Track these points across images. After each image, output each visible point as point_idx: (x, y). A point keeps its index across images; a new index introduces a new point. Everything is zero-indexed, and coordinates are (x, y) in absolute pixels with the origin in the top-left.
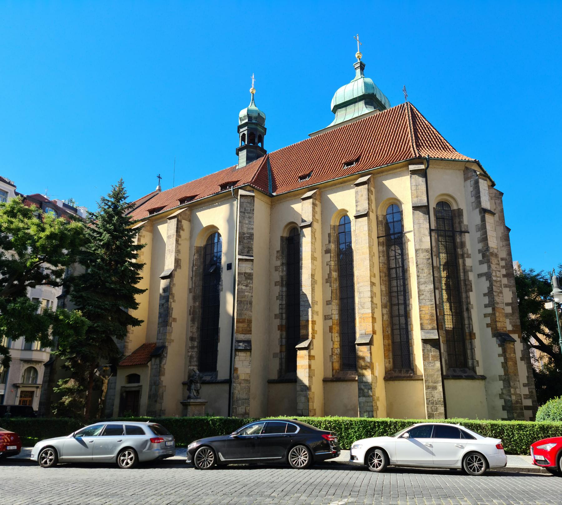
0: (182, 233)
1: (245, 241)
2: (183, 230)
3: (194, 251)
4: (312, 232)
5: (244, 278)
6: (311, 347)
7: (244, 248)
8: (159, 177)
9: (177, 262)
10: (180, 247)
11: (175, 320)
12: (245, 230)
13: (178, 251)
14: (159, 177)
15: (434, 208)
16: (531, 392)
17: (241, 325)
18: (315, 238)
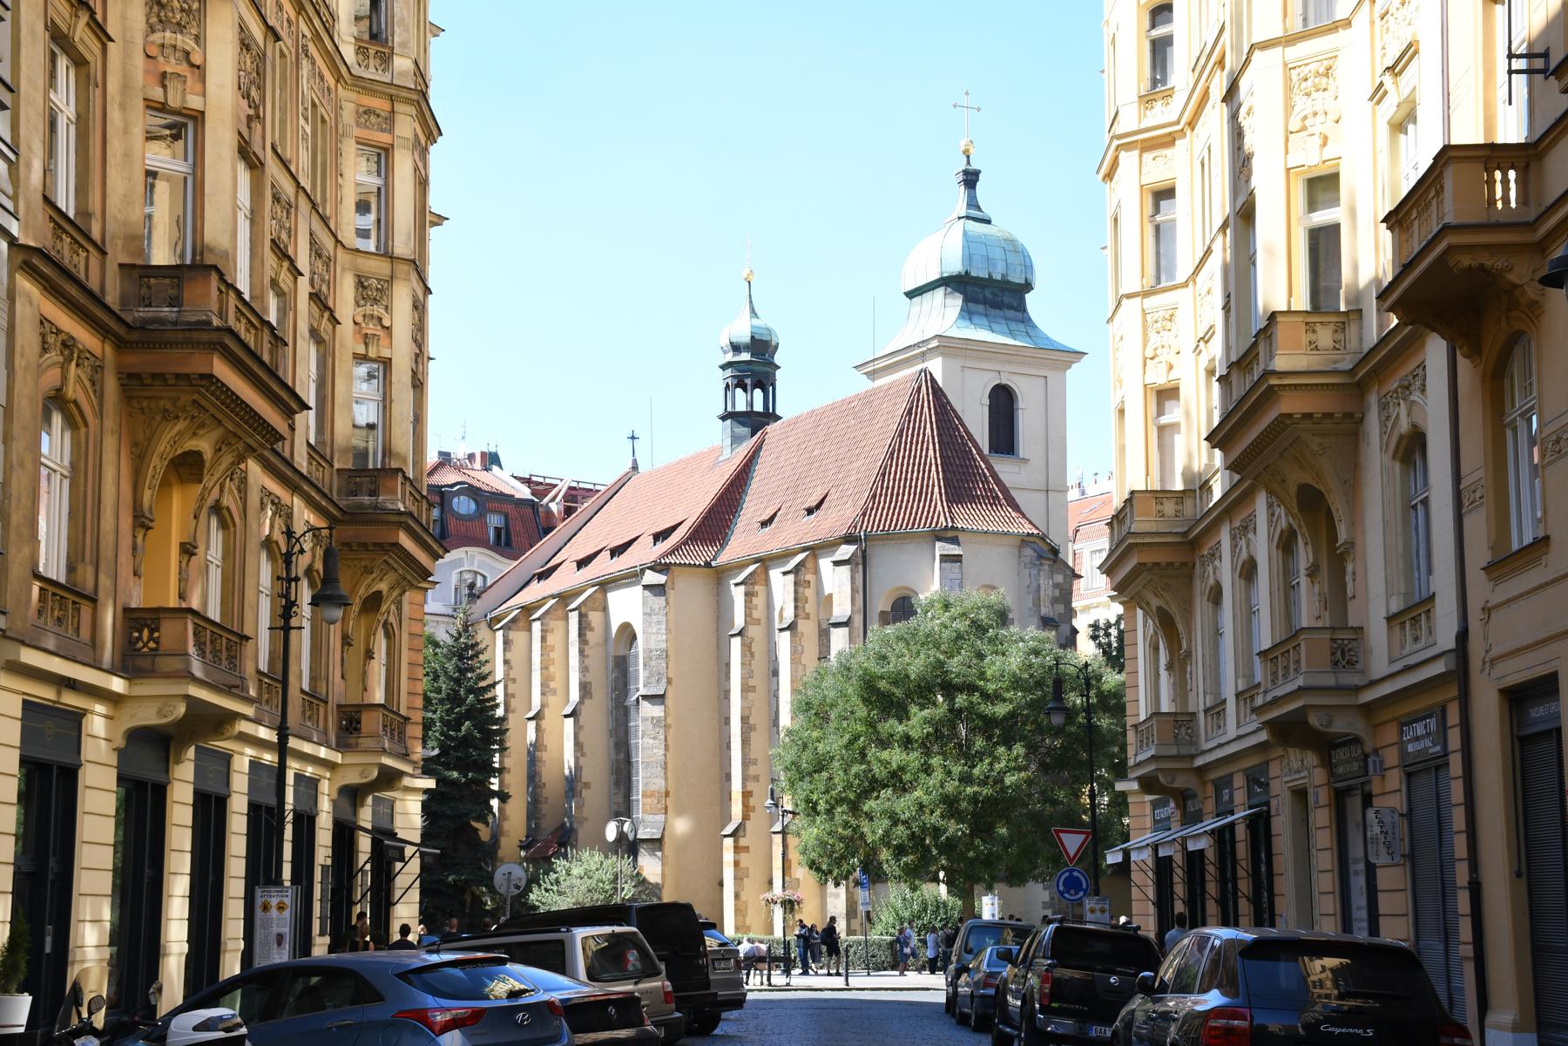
0: (589, 635)
1: (653, 663)
2: (592, 630)
3: (611, 664)
4: (743, 644)
5: (650, 726)
6: (741, 833)
7: (651, 675)
8: (633, 438)
9: (585, 688)
10: (587, 661)
11: (587, 785)
12: (653, 646)
13: (584, 669)
14: (633, 438)
15: (883, 612)
16: (1052, 898)
17: (648, 800)
18: (752, 654)
